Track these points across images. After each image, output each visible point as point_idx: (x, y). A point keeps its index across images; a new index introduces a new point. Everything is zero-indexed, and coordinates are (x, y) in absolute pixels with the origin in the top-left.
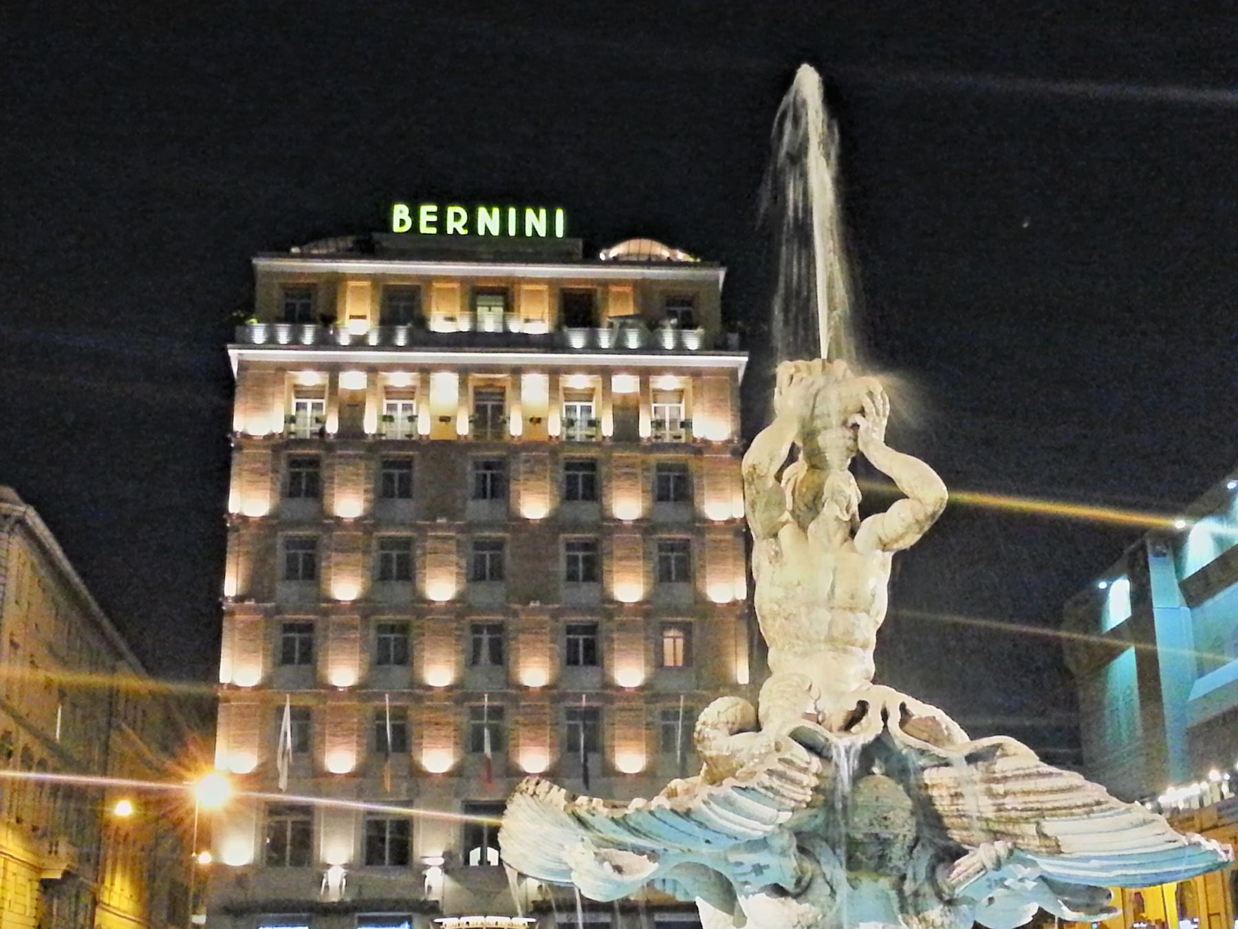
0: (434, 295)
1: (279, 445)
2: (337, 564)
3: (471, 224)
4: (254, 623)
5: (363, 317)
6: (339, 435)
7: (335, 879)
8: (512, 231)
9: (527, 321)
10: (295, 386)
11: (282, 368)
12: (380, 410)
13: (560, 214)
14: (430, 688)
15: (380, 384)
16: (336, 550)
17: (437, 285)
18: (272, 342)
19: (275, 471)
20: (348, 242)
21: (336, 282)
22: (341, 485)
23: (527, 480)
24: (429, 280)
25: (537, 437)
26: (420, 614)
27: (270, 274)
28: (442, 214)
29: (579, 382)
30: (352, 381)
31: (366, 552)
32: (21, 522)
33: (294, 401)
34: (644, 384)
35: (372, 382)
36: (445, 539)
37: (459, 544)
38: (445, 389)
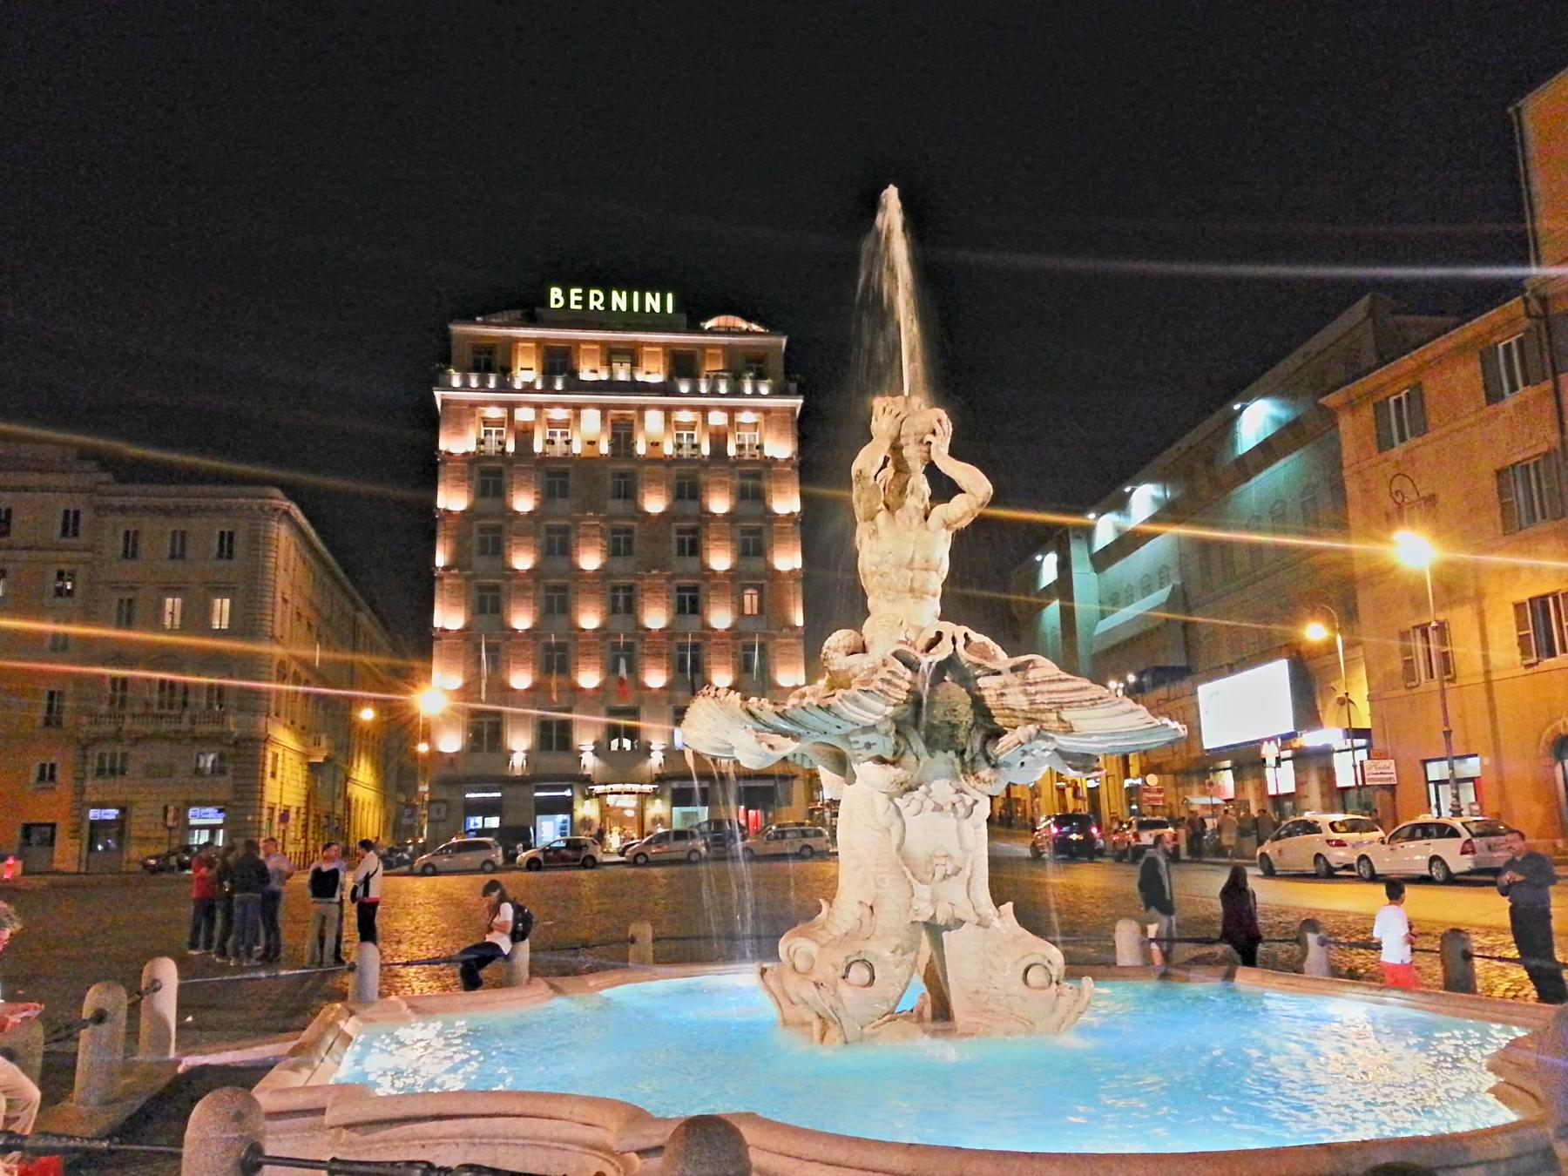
0: (581, 354)
1: (470, 459)
3: (607, 303)
7: (518, 760)
8: (636, 309)
9: (648, 373)
11: (474, 405)
12: (544, 435)
13: (670, 297)
14: (584, 630)
15: (544, 417)
17: (583, 347)
18: (466, 386)
20: (518, 313)
21: (510, 344)
22: (518, 489)
24: (578, 342)
25: (655, 454)
29: (685, 416)
30: (524, 415)
31: (537, 536)
33: (483, 429)
34: (731, 419)
35: (538, 416)
36: (592, 526)
38: (591, 422)
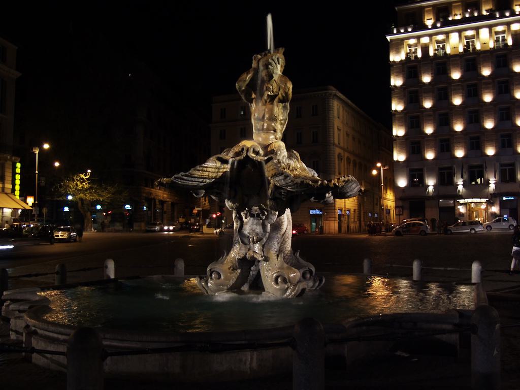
2: (424, 97)
7: (431, 189)
10: (408, 44)
11: (403, 40)
16: (424, 93)
18: (399, 32)
19: (403, 71)
29: (500, 28)
32: (335, 95)
35: (431, 40)
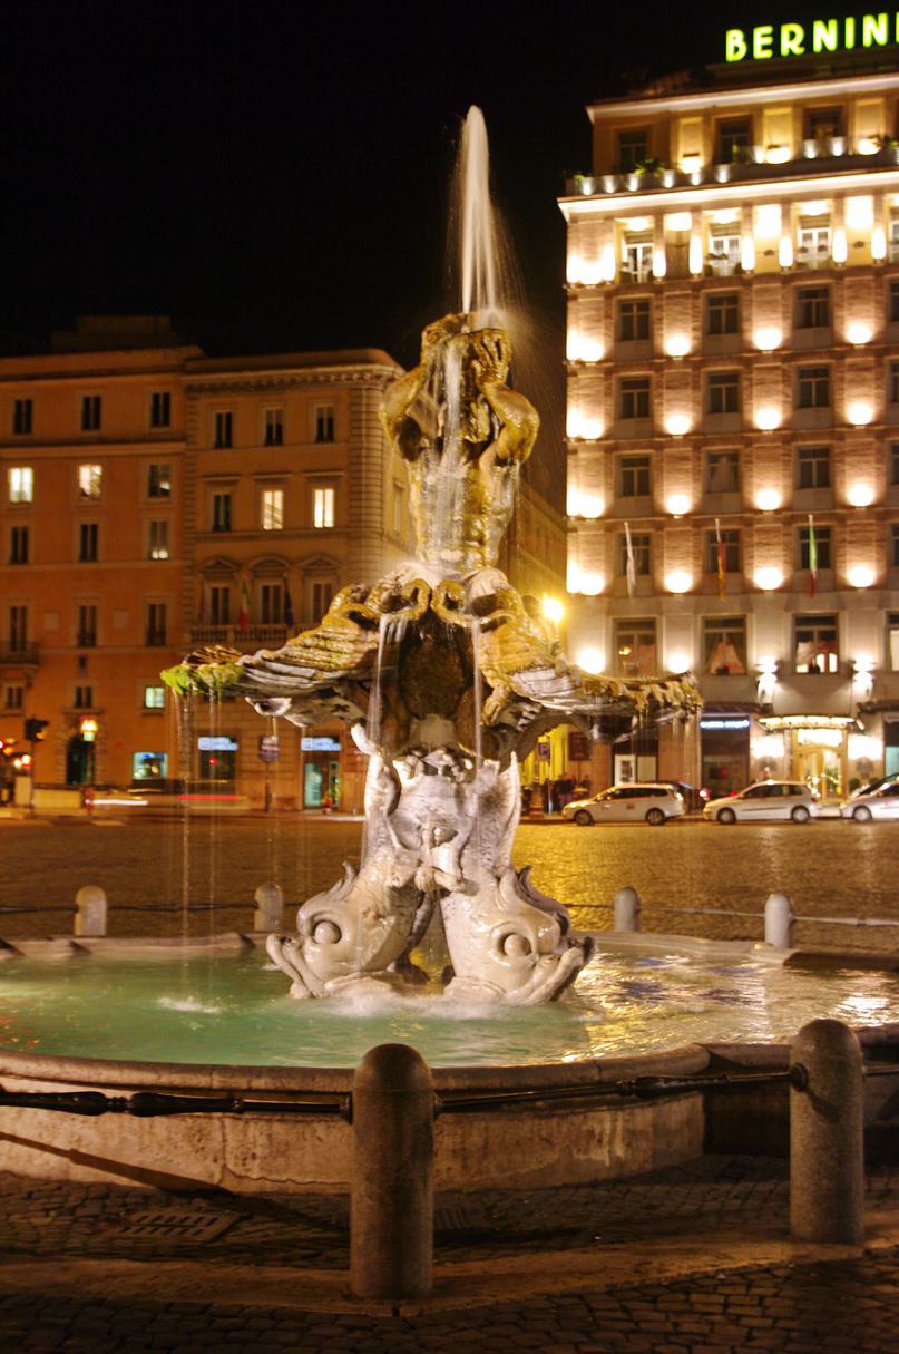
0: (766, 122)
1: (606, 292)
2: (668, 401)
3: (808, 42)
4: (596, 460)
5: (696, 155)
6: (667, 277)
10: (625, 233)
16: (668, 388)
17: (768, 112)
19: (608, 316)
21: (668, 122)
22: (670, 325)
23: (851, 305)
24: (758, 109)
25: (861, 259)
26: (749, 442)
27: (605, 121)
28: (776, 35)
31: (696, 387)
35: (696, 222)
37: (785, 372)
